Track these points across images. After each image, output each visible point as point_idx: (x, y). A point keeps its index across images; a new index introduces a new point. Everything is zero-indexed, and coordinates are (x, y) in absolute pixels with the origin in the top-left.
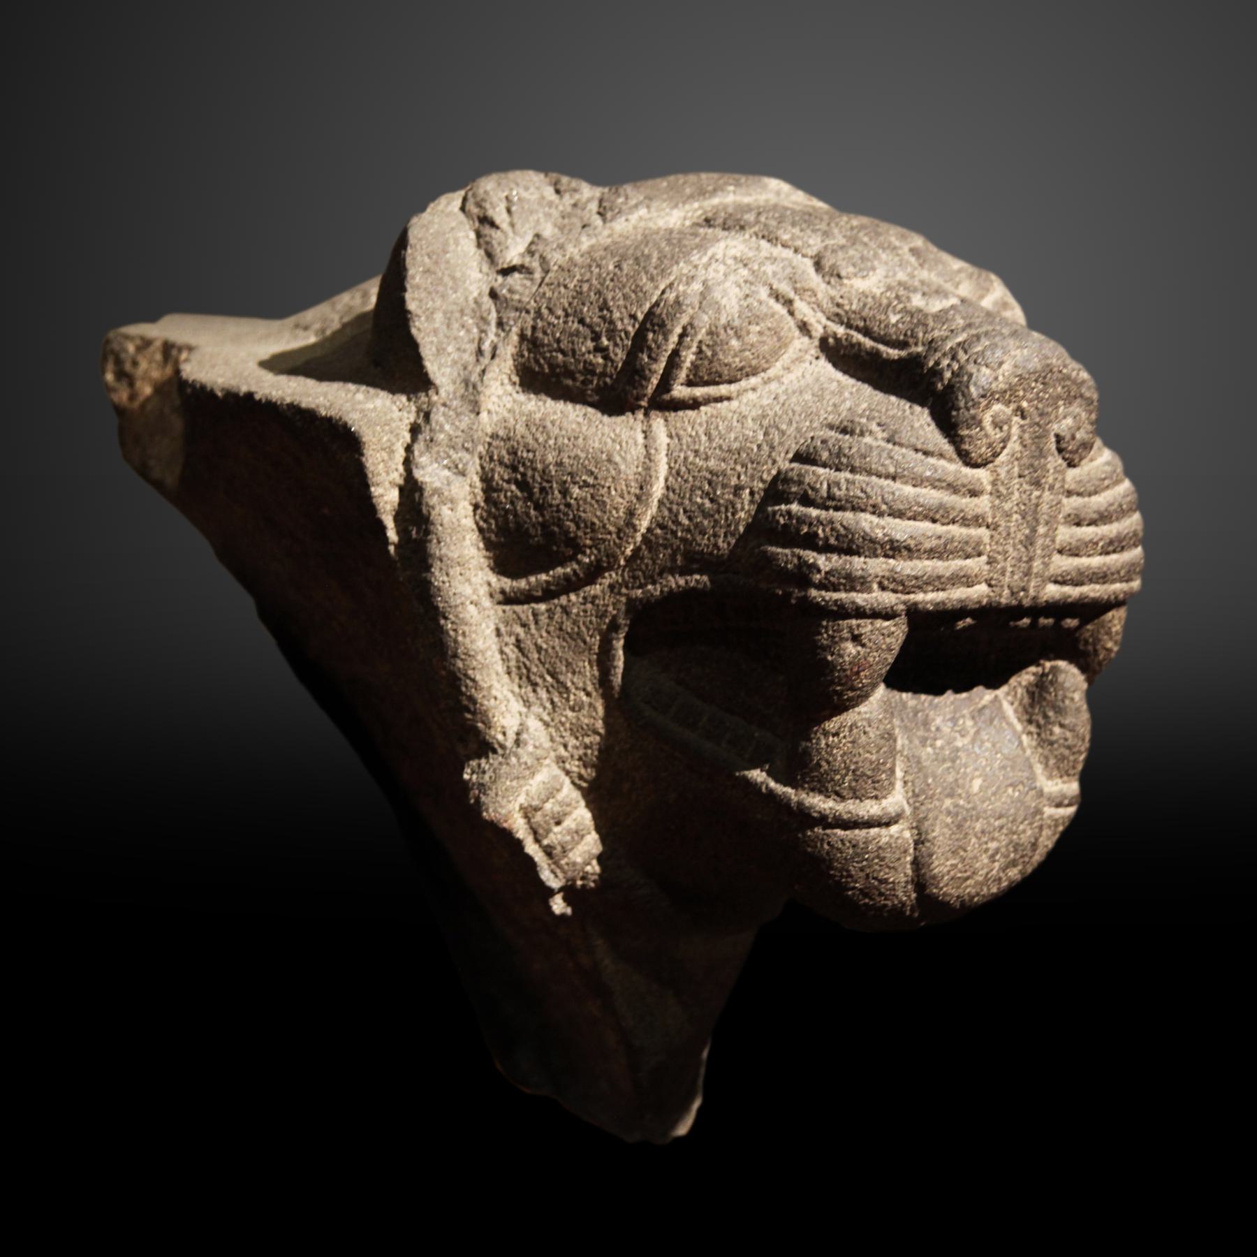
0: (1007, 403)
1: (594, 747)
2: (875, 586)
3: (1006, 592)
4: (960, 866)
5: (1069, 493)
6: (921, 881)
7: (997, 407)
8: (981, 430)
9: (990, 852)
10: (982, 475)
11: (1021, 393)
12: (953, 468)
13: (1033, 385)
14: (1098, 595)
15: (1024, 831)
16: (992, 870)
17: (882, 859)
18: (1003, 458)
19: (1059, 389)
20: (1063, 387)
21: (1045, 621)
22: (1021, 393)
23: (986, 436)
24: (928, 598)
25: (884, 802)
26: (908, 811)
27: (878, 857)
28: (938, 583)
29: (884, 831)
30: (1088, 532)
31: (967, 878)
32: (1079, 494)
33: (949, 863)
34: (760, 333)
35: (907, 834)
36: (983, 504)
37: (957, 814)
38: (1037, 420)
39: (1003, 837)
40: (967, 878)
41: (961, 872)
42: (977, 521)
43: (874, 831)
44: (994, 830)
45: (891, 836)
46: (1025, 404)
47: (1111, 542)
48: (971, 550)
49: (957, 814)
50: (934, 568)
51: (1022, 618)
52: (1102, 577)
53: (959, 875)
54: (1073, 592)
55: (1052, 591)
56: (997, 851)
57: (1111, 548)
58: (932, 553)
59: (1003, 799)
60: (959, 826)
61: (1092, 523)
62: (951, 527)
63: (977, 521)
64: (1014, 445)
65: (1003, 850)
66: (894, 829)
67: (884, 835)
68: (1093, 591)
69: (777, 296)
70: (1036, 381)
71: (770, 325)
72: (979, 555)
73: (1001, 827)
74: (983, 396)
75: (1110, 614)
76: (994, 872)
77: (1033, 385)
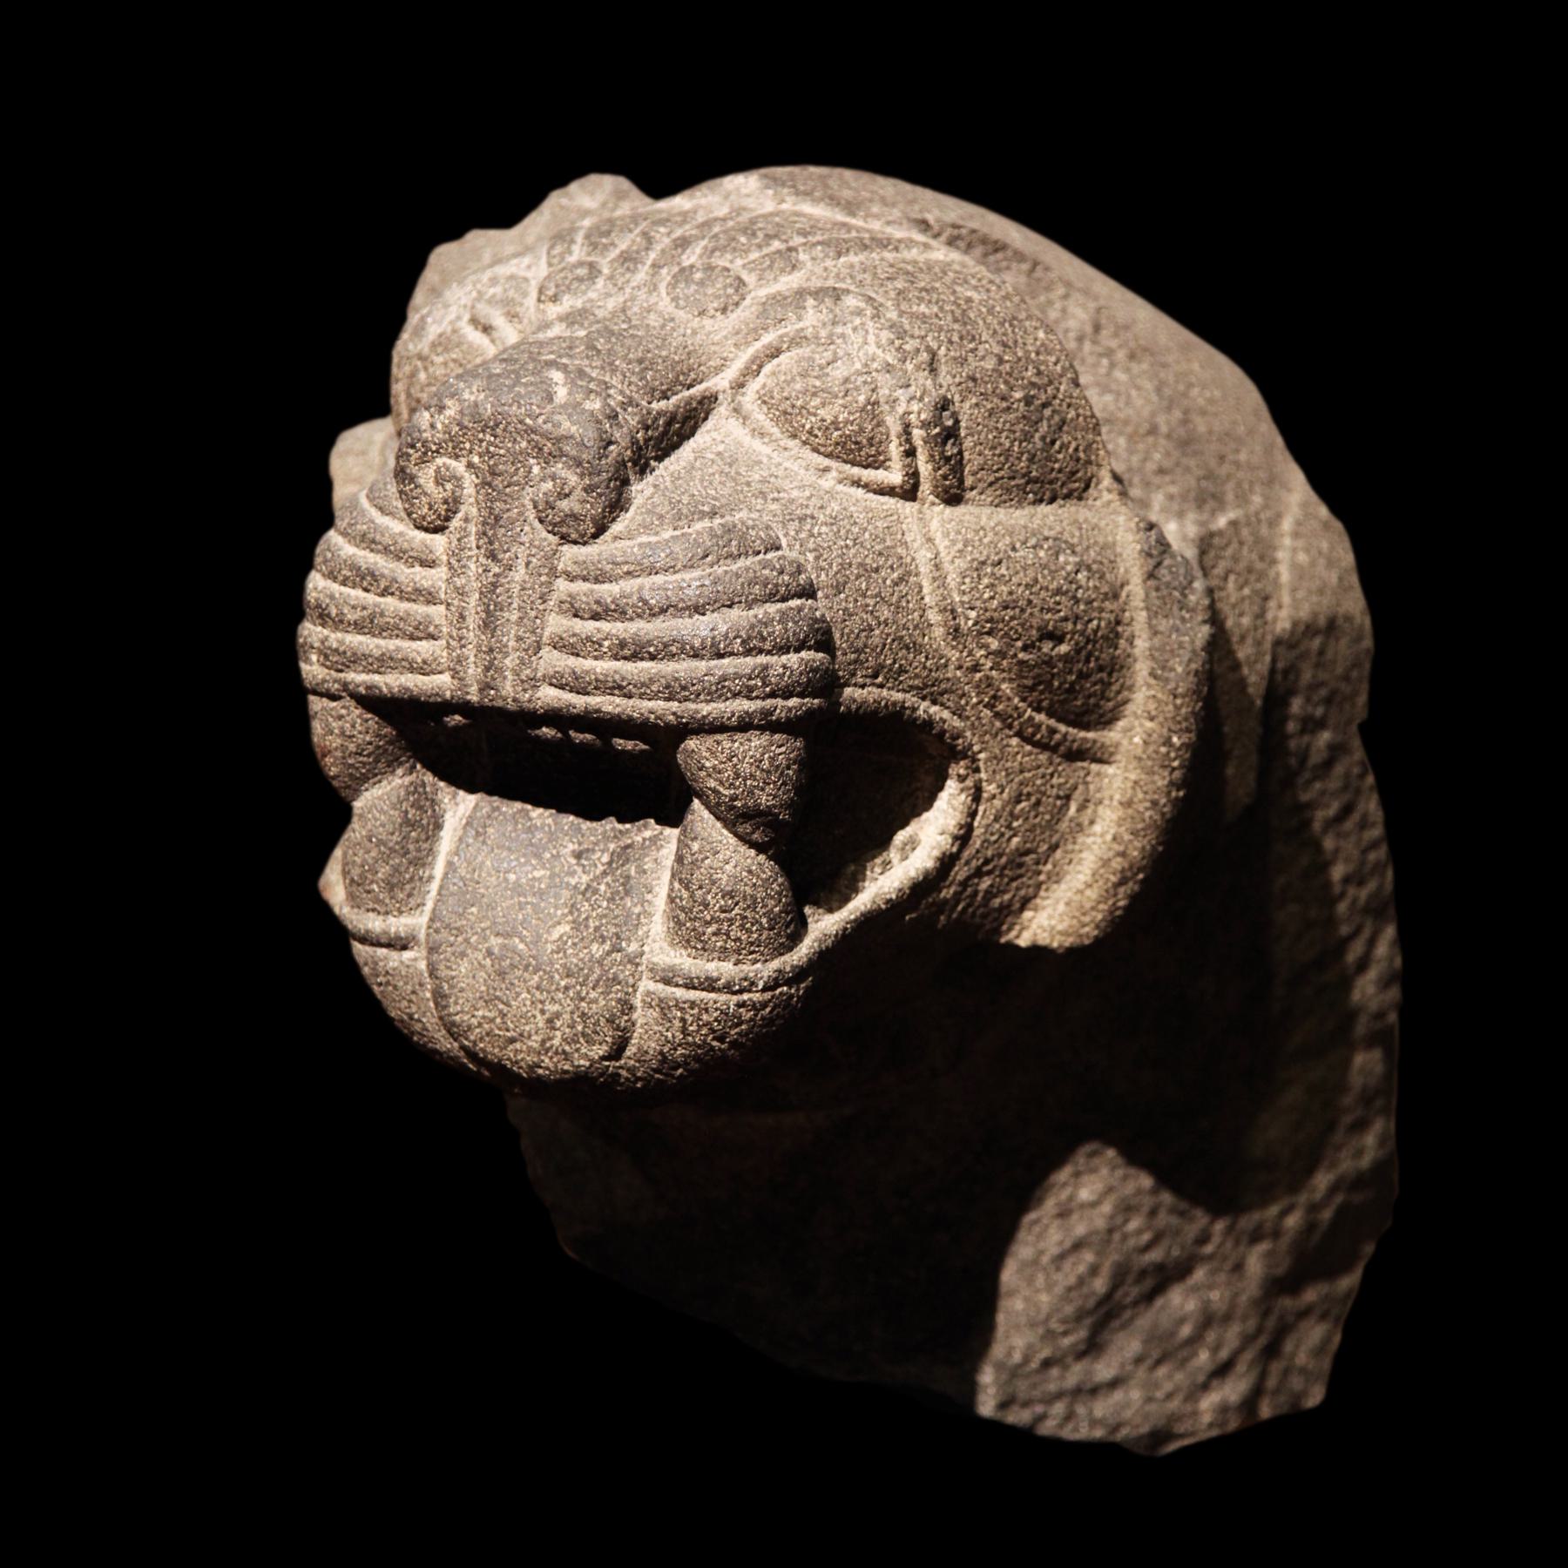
0: (457, 457)
1: (1073, 904)
2: (314, 658)
3: (474, 689)
4: (498, 1020)
5: (572, 578)
6: (452, 1029)
7: (440, 461)
8: (416, 487)
9: (547, 1015)
10: (439, 543)
11: (467, 445)
12: (397, 527)
13: (481, 436)
14: (617, 710)
15: (595, 1001)
16: (550, 1039)
17: (395, 987)
18: (455, 523)
19: (524, 444)
20: (529, 442)
21: (578, 737)
22: (467, 445)
23: (426, 494)
24: (391, 682)
25: (391, 920)
26: (422, 936)
27: (388, 983)
28: (383, 663)
29: (394, 955)
30: (589, 627)
31: (512, 1041)
32: (585, 579)
33: (480, 1013)
34: (445, 364)
35: (422, 965)
36: (435, 578)
37: (502, 958)
38: (489, 479)
39: (569, 1001)
40: (512, 1041)
41: (500, 1029)
42: (430, 598)
43: (382, 952)
44: (558, 989)
45: (402, 962)
46: (476, 459)
47: (623, 644)
48: (423, 632)
49: (502, 958)
50: (361, 643)
51: (540, 728)
52: (617, 688)
53: (497, 1032)
54: (579, 702)
55: (549, 696)
56: (558, 1015)
57: (627, 652)
58: (359, 627)
59: (581, 955)
60: (502, 974)
61: (595, 617)
62: (389, 599)
63: (430, 598)
64: (469, 508)
65: (567, 1016)
66: (407, 955)
67: (393, 959)
68: (610, 704)
69: (474, 321)
70: (483, 431)
71: (454, 356)
72: (433, 637)
73: (567, 988)
74: (413, 446)
75: (692, 743)
76: (556, 1042)
77: (481, 436)
